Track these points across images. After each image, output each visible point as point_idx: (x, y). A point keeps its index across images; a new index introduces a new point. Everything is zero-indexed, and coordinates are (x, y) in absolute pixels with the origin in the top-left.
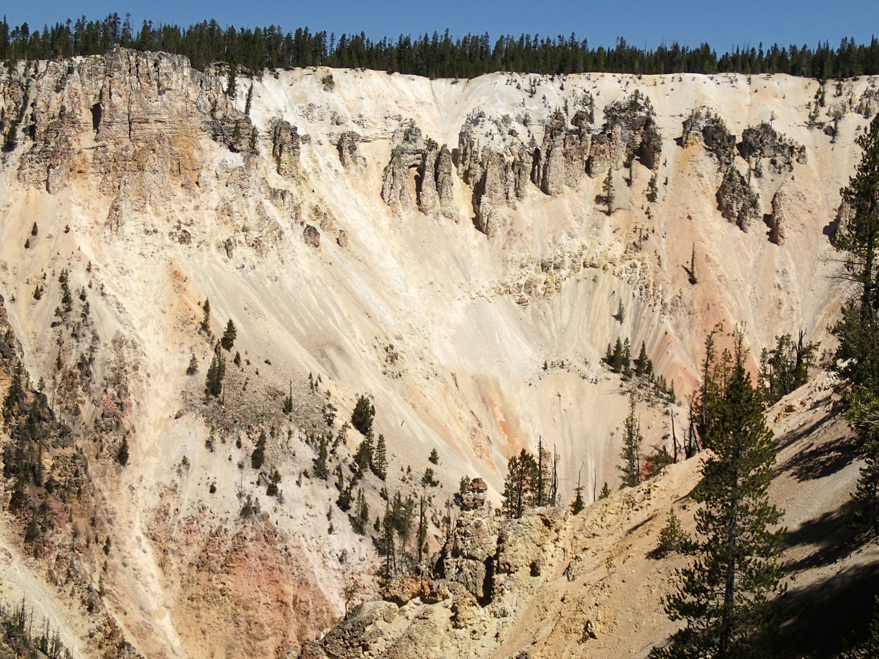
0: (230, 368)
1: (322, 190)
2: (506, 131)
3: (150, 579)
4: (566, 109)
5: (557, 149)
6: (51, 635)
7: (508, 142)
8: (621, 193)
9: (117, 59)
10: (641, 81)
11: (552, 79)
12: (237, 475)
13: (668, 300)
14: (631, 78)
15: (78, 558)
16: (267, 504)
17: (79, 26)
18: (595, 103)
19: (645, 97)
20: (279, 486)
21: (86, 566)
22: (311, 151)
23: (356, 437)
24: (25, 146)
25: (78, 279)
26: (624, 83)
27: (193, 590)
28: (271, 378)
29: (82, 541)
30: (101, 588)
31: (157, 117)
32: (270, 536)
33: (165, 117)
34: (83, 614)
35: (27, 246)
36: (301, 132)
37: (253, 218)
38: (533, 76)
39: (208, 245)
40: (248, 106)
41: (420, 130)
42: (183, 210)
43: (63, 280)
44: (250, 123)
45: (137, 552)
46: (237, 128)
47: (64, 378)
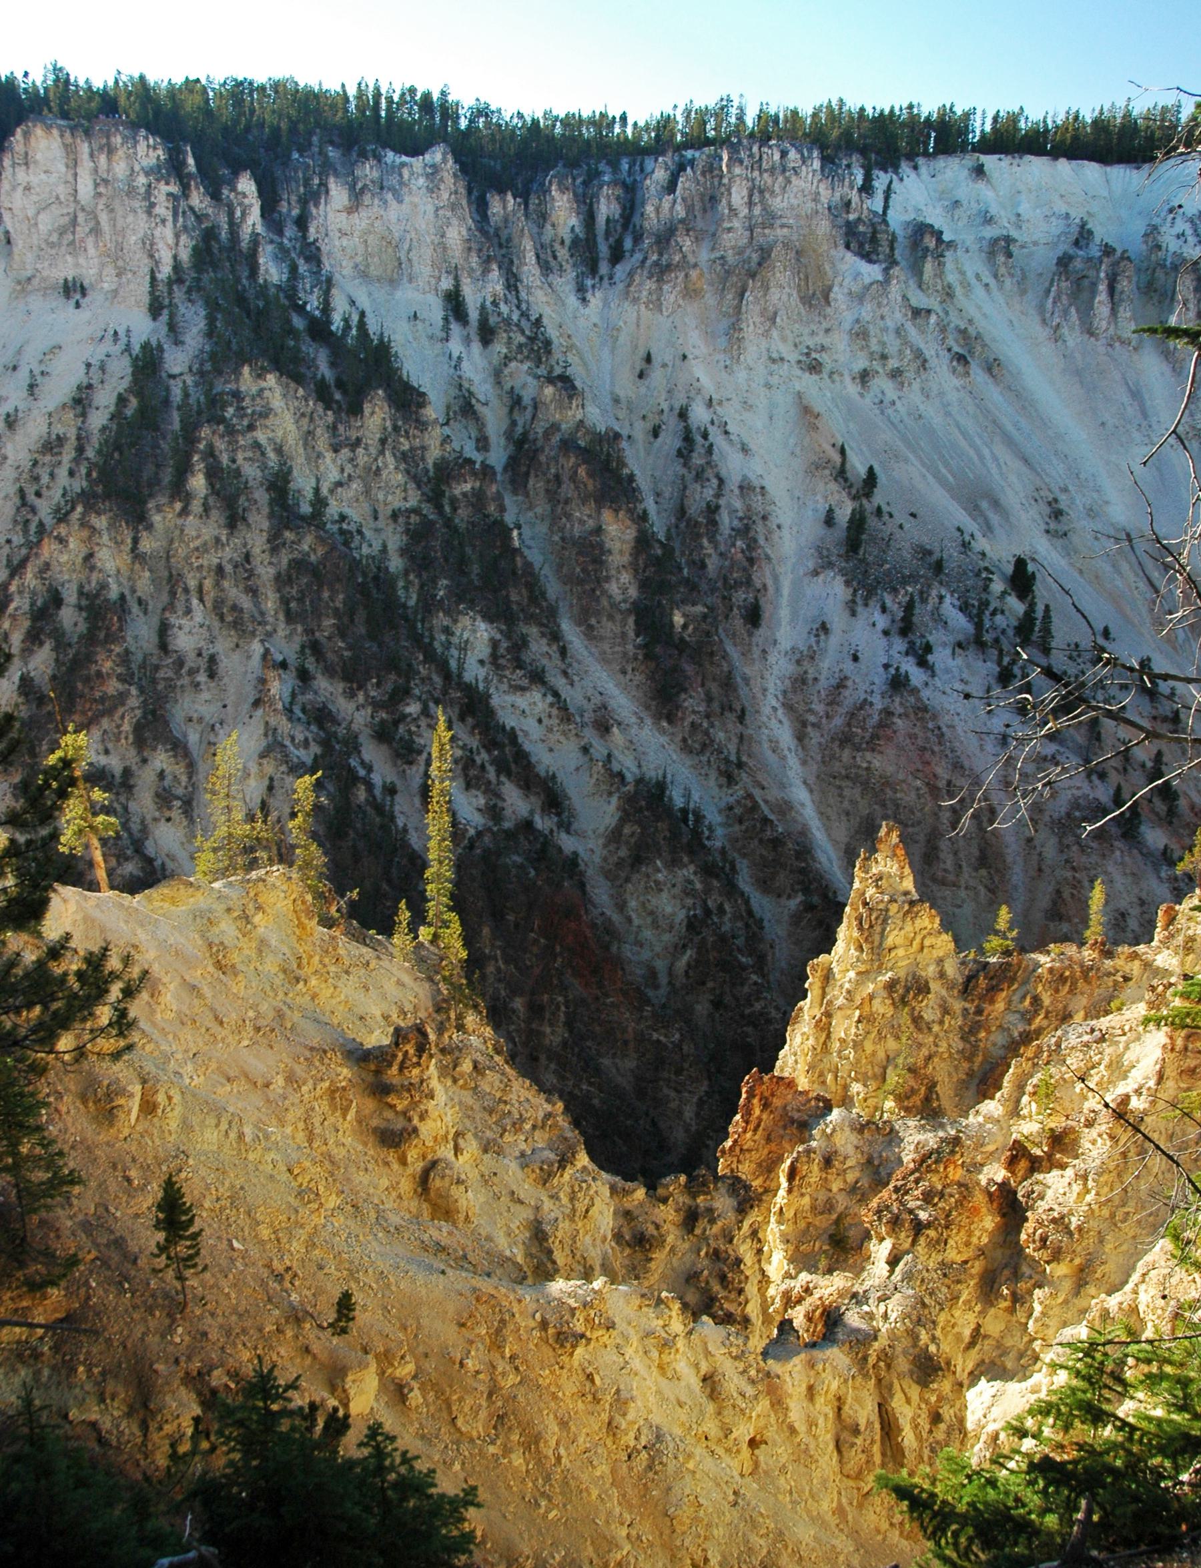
0: (872, 522)
1: (972, 311)
3: (786, 752)
6: (692, 805)
9: (738, 152)
12: (882, 642)
15: (713, 726)
16: (917, 676)
17: (687, 113)
20: (930, 657)
21: (721, 736)
22: (956, 261)
23: (1016, 606)
24: (633, 260)
25: (699, 415)
27: (837, 767)
28: (912, 535)
29: (716, 706)
30: (739, 758)
31: (784, 221)
32: (922, 711)
34: (720, 786)
35: (641, 375)
36: (946, 237)
37: (893, 345)
40: (886, 207)
42: (813, 333)
43: (683, 414)
44: (887, 225)
45: (774, 723)
46: (875, 232)
47: (687, 526)
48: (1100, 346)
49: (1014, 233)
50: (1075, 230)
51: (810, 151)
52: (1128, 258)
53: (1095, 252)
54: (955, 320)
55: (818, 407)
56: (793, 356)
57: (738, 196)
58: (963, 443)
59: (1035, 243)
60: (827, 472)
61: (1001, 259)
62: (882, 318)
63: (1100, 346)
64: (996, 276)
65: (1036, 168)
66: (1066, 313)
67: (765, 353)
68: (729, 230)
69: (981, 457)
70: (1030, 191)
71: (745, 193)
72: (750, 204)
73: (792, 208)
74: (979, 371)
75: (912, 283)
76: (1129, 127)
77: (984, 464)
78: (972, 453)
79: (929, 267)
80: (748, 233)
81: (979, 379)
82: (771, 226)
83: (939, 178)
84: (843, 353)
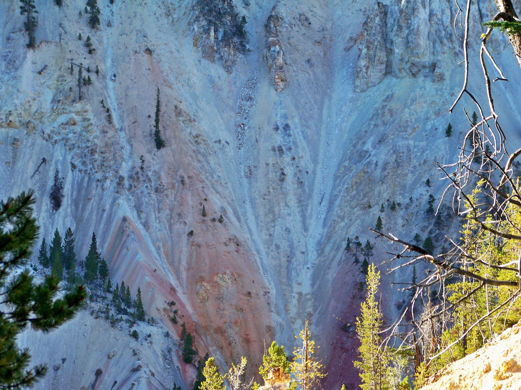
13: (124, 171)
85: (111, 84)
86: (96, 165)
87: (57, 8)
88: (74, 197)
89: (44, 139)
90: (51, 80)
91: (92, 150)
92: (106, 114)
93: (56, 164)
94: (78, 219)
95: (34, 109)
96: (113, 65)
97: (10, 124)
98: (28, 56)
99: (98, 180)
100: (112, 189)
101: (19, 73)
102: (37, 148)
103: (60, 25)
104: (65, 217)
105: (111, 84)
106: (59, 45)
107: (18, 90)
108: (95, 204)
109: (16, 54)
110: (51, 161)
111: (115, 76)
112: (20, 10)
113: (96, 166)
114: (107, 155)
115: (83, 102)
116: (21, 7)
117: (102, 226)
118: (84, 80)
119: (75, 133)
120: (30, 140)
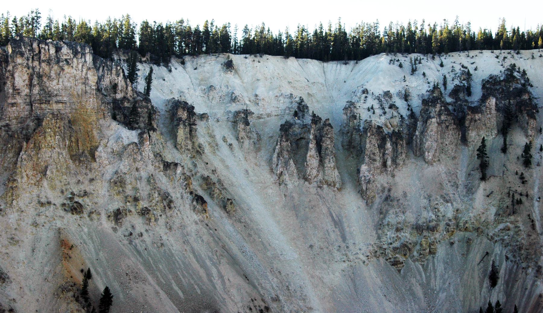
1: (216, 163)
2: (386, 106)
4: (445, 84)
5: (434, 120)
7: (388, 116)
8: (496, 160)
10: (519, 56)
11: (433, 58)
14: (509, 53)
18: (474, 77)
19: (521, 70)
26: (501, 58)
31: (59, 98)
33: (65, 99)
36: (198, 110)
37: (144, 189)
38: (414, 56)
39: (99, 214)
41: (307, 107)
48: (312, 188)
49: (252, 109)
50: (295, 105)
51: (83, 48)
52: (330, 125)
53: (308, 120)
54: (202, 171)
55: (74, 240)
56: (58, 200)
57: (20, 79)
58: (196, 265)
59: (269, 115)
60: (71, 294)
61: (241, 126)
62: (137, 170)
63: (312, 188)
64: (237, 139)
65: (272, 64)
66: (286, 164)
67: (36, 198)
68: (13, 105)
69: (209, 275)
70: (266, 79)
71: (26, 77)
72: (31, 85)
73: (66, 89)
74: (218, 209)
75: (170, 144)
76: (341, 37)
77: (211, 281)
78: (202, 272)
79: (181, 133)
80: (28, 108)
81: (216, 214)
82: (48, 102)
83: (200, 70)
84: (103, 197)
85: (536, 204)
86: (522, 257)
87: (503, 155)
88: (506, 278)
89: (488, 239)
90: (495, 200)
91: (520, 247)
92: (531, 223)
93: (496, 256)
94: (508, 294)
95: (483, 219)
96: (539, 191)
97: (466, 229)
98: (481, 185)
99: (523, 268)
100: (533, 274)
101: (474, 196)
102: (483, 245)
103: (504, 165)
104: (499, 292)
105: (536, 204)
106: (502, 178)
107: (473, 208)
108: (520, 284)
109: (474, 184)
110: (492, 254)
111: (539, 198)
112: (476, 157)
113: (522, 258)
114: (530, 251)
115: (516, 215)
116: (478, 155)
117: (524, 300)
118: (517, 200)
119: (509, 236)
120: (479, 240)
